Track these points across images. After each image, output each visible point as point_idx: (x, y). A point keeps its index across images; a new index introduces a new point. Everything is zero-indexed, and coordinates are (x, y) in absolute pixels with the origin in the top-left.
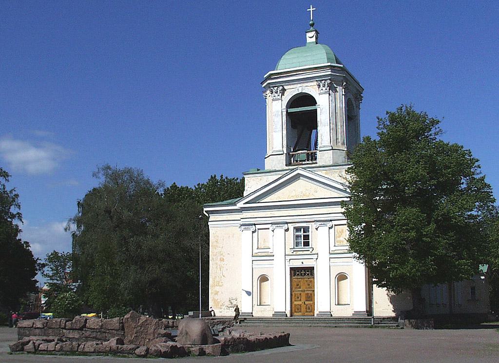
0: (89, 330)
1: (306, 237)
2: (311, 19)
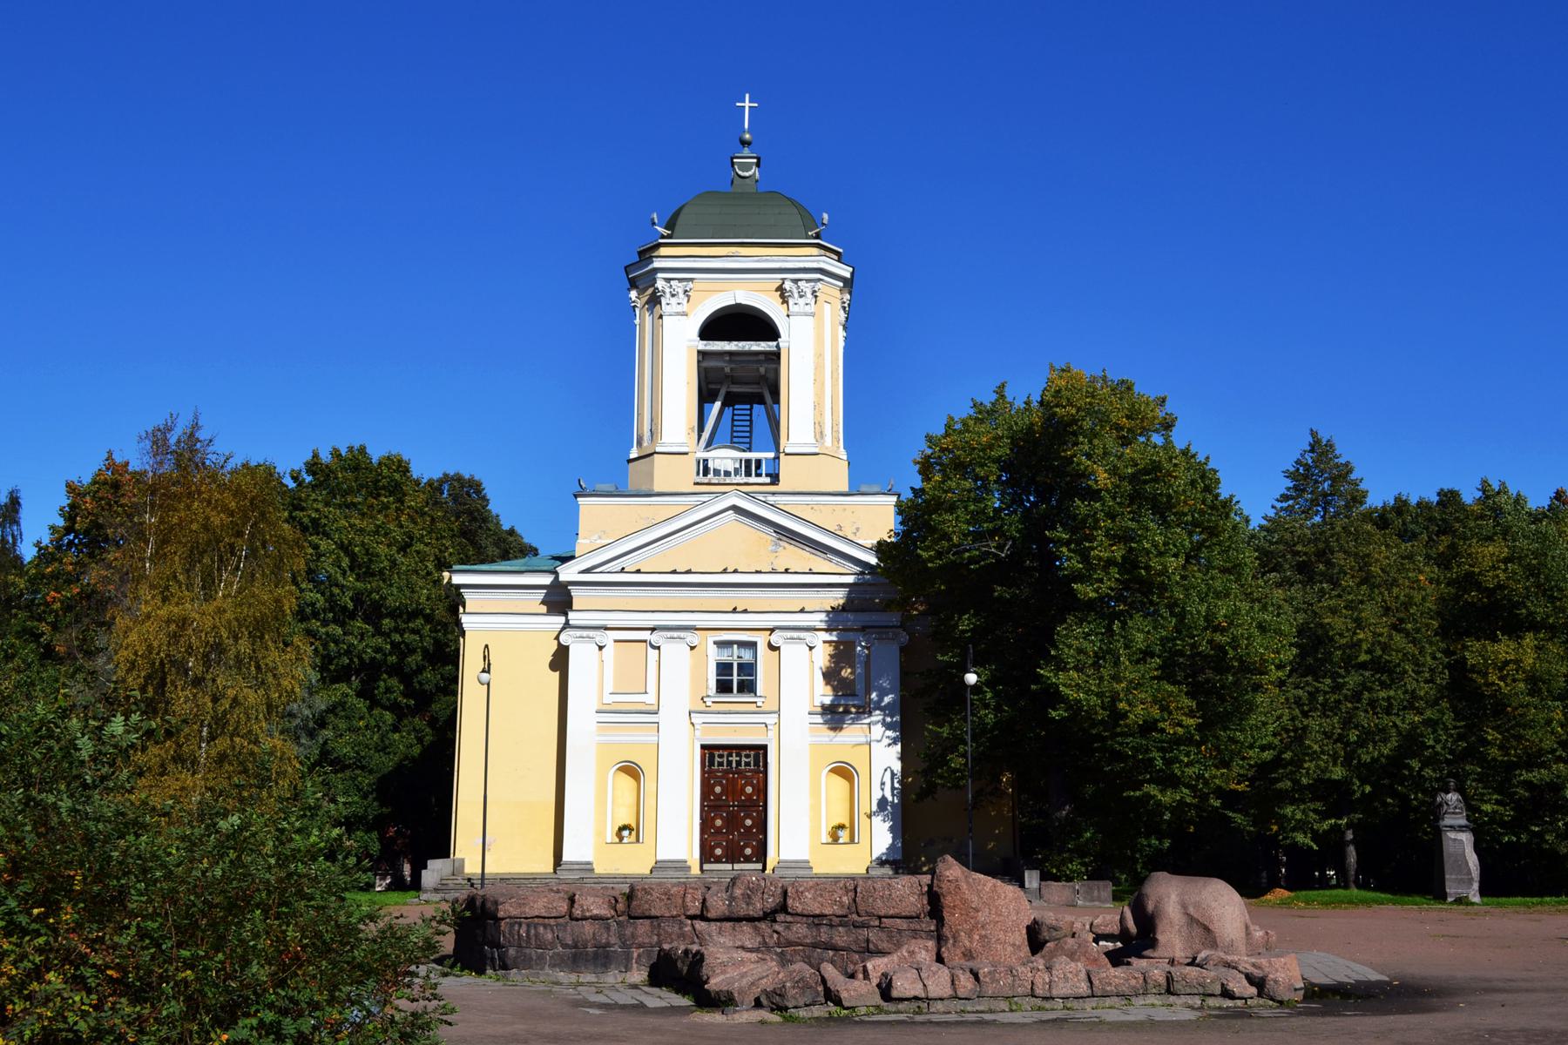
0: (799, 919)
1: (748, 669)
2: (746, 126)
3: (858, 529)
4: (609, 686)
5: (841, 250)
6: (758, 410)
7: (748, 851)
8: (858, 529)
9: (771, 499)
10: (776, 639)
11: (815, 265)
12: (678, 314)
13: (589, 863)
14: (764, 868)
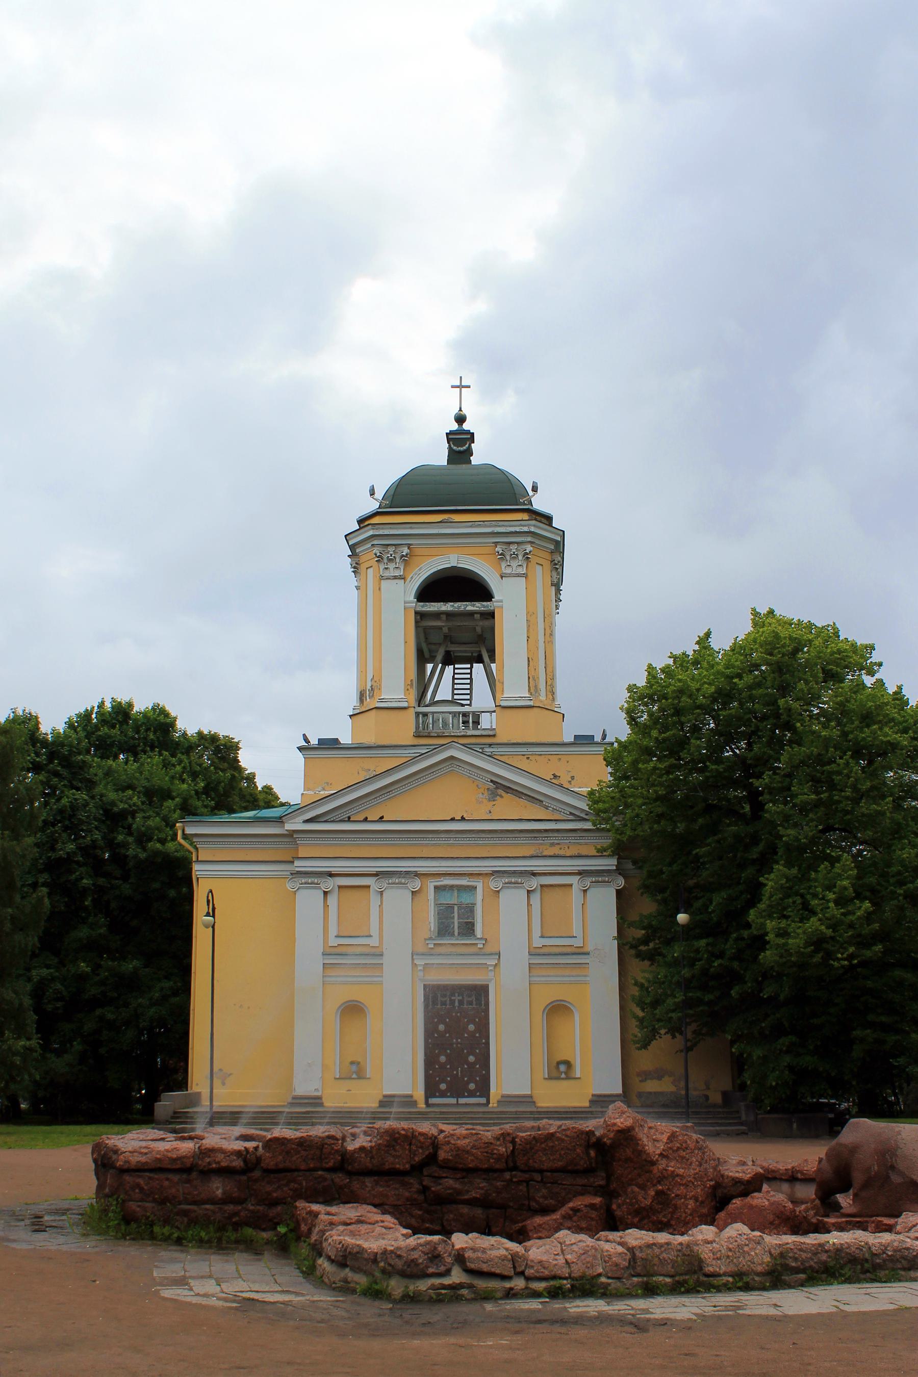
3: (573, 778)
4: (333, 930)
6: (478, 668)
7: (472, 1086)
8: (573, 778)
9: (488, 750)
11: (526, 529)
12: (395, 578)
13: (320, 1098)
14: (488, 1102)
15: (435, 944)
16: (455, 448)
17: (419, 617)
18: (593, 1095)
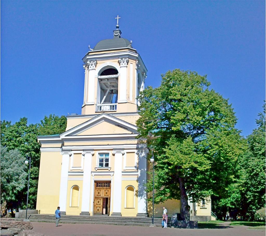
1: (107, 160)
2: (118, 23)
5: (136, 50)
10: (113, 152)
12: (93, 69)
13: (65, 212)
15: (98, 169)
16: (115, 35)
17: (100, 81)
18: (138, 213)
